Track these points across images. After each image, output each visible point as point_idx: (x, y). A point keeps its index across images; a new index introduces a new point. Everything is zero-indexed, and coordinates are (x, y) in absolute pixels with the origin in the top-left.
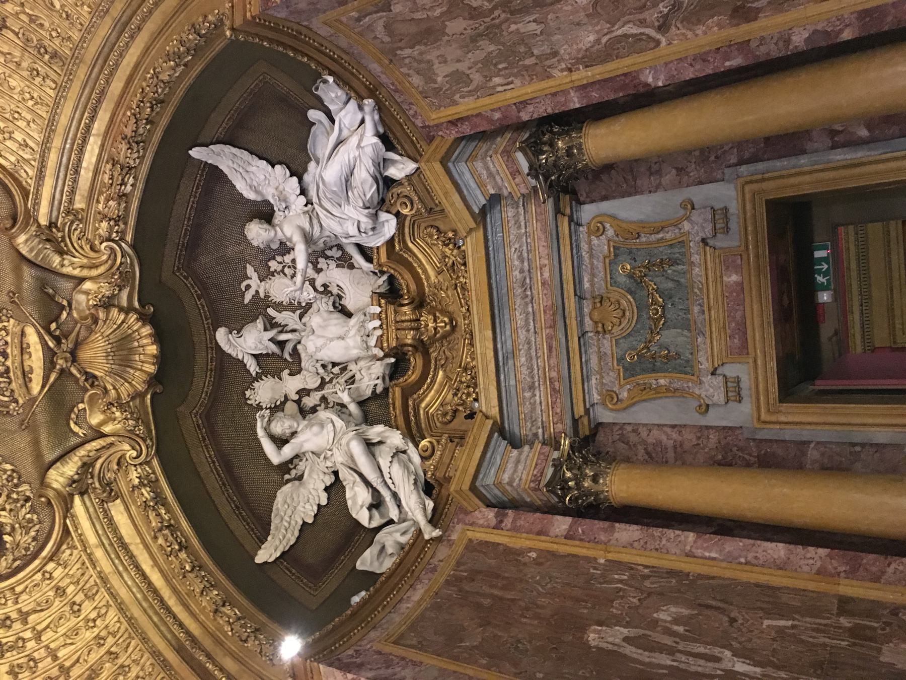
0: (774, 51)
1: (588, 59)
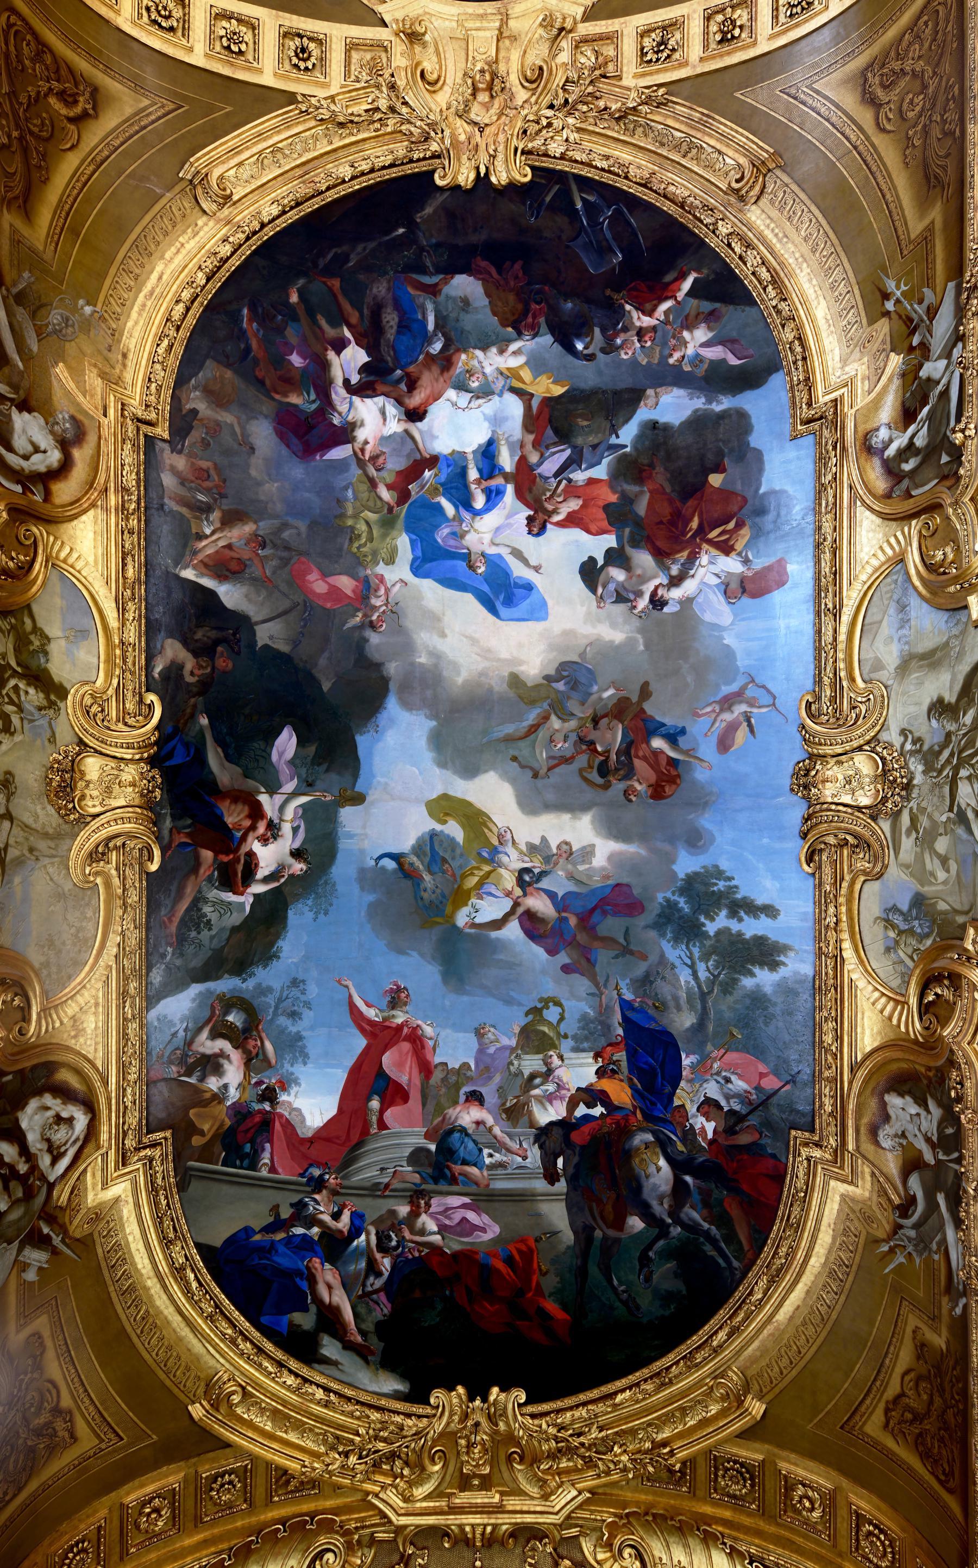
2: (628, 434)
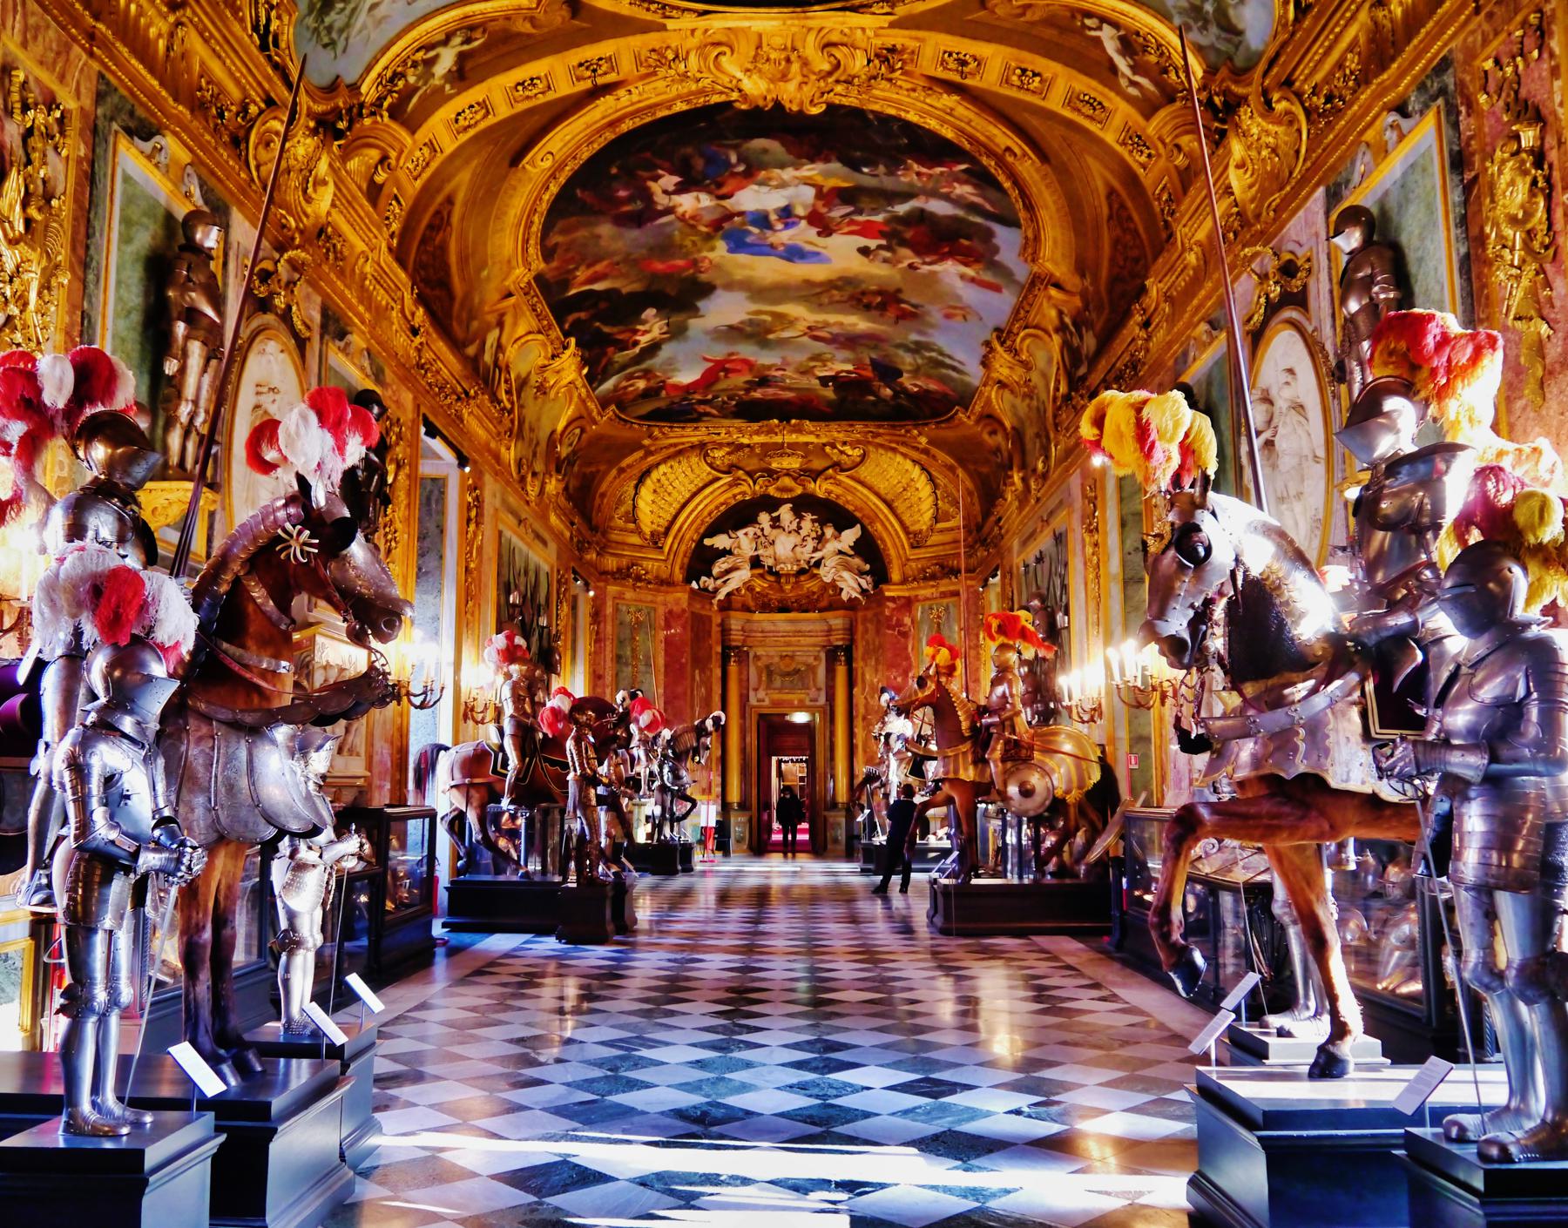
2: (902, 209)
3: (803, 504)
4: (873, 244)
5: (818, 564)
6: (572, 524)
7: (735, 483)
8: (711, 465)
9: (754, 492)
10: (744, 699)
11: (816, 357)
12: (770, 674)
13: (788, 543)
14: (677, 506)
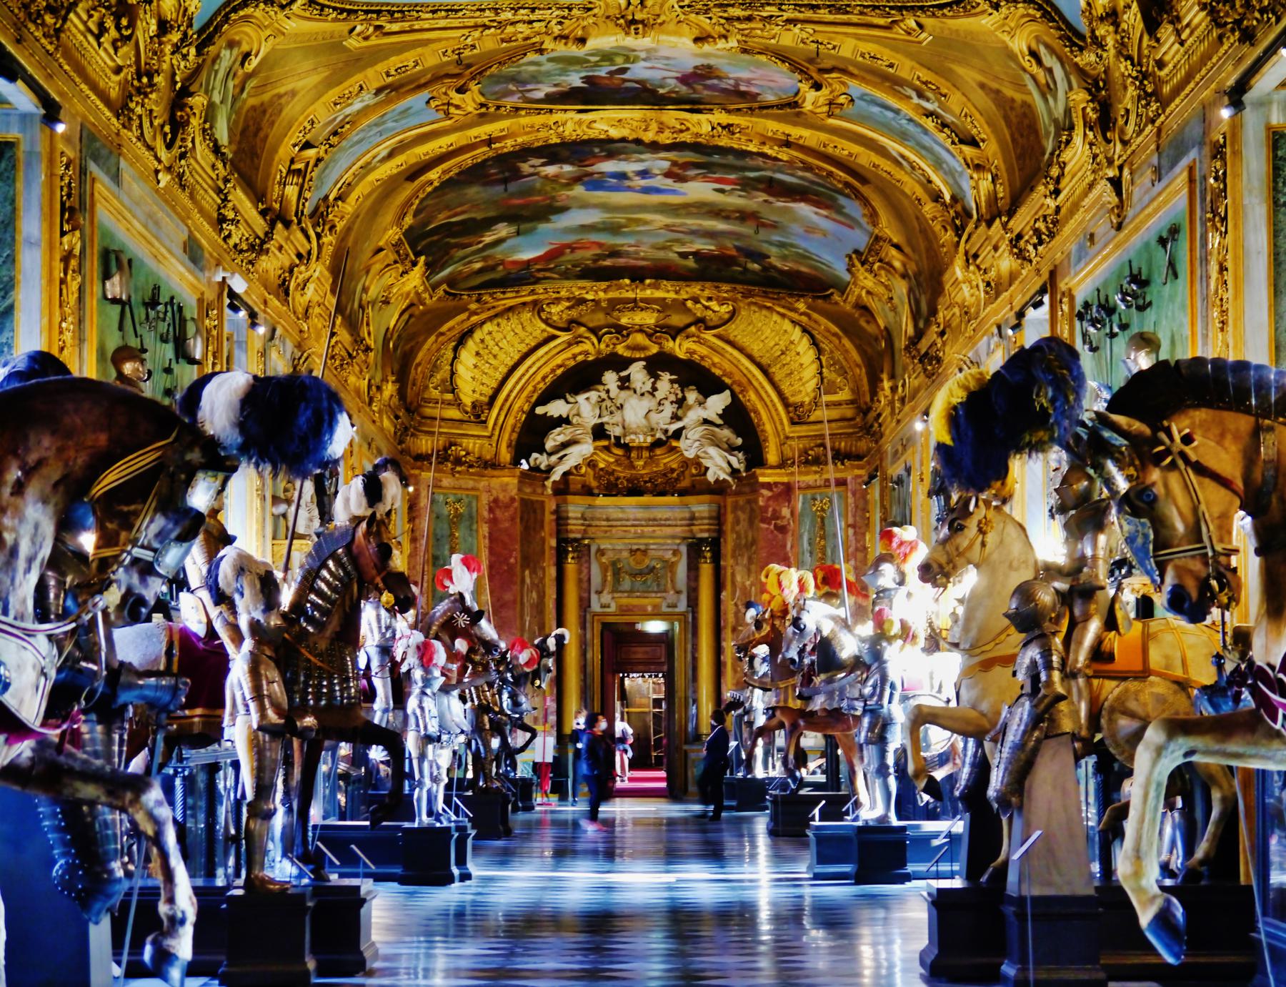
0: (723, 636)
1: (733, 575)
2: (752, 175)
3: (656, 365)
4: (728, 188)
5: (678, 434)
6: (397, 417)
7: (577, 341)
8: (546, 322)
9: (599, 352)
10: (584, 604)
11: (677, 241)
12: (617, 573)
13: (639, 408)
14: (504, 370)
